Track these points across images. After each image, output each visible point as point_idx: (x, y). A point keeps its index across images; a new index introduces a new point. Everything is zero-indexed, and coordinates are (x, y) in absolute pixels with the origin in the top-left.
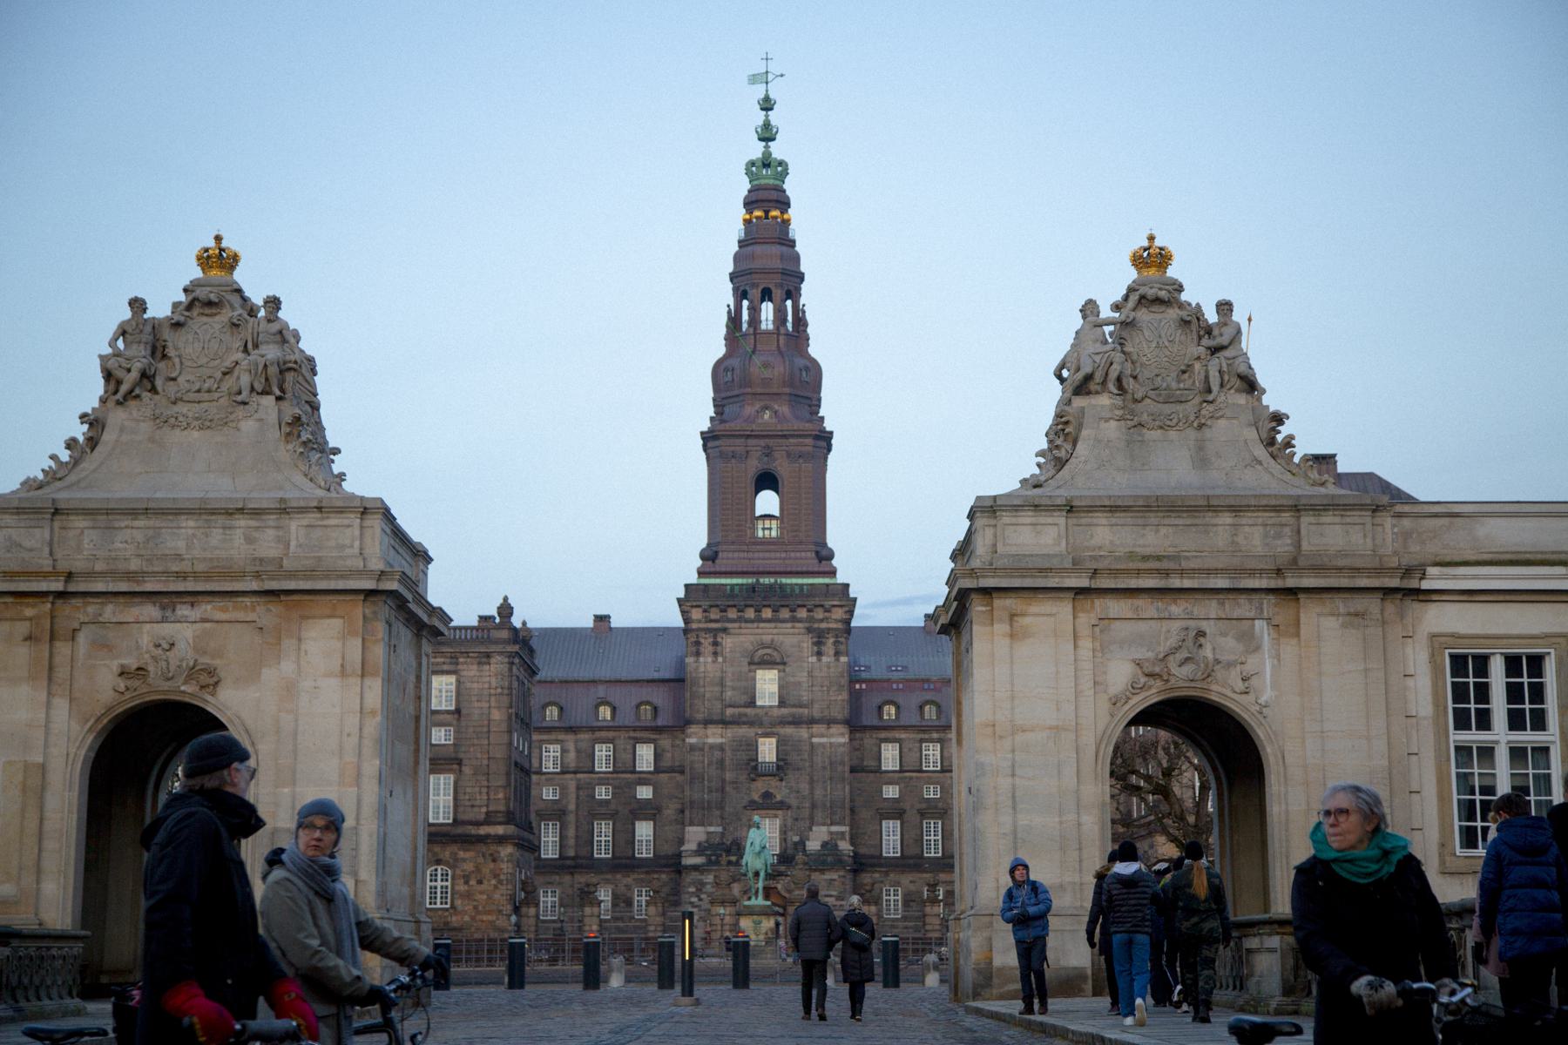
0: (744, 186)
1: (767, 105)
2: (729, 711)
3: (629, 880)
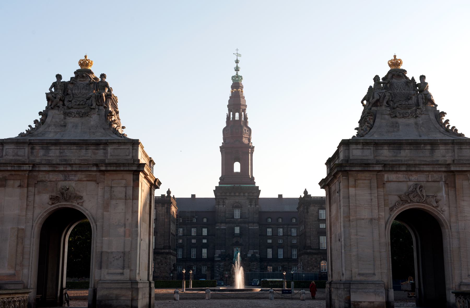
0: (231, 82)
1: (237, 62)
2: (227, 220)
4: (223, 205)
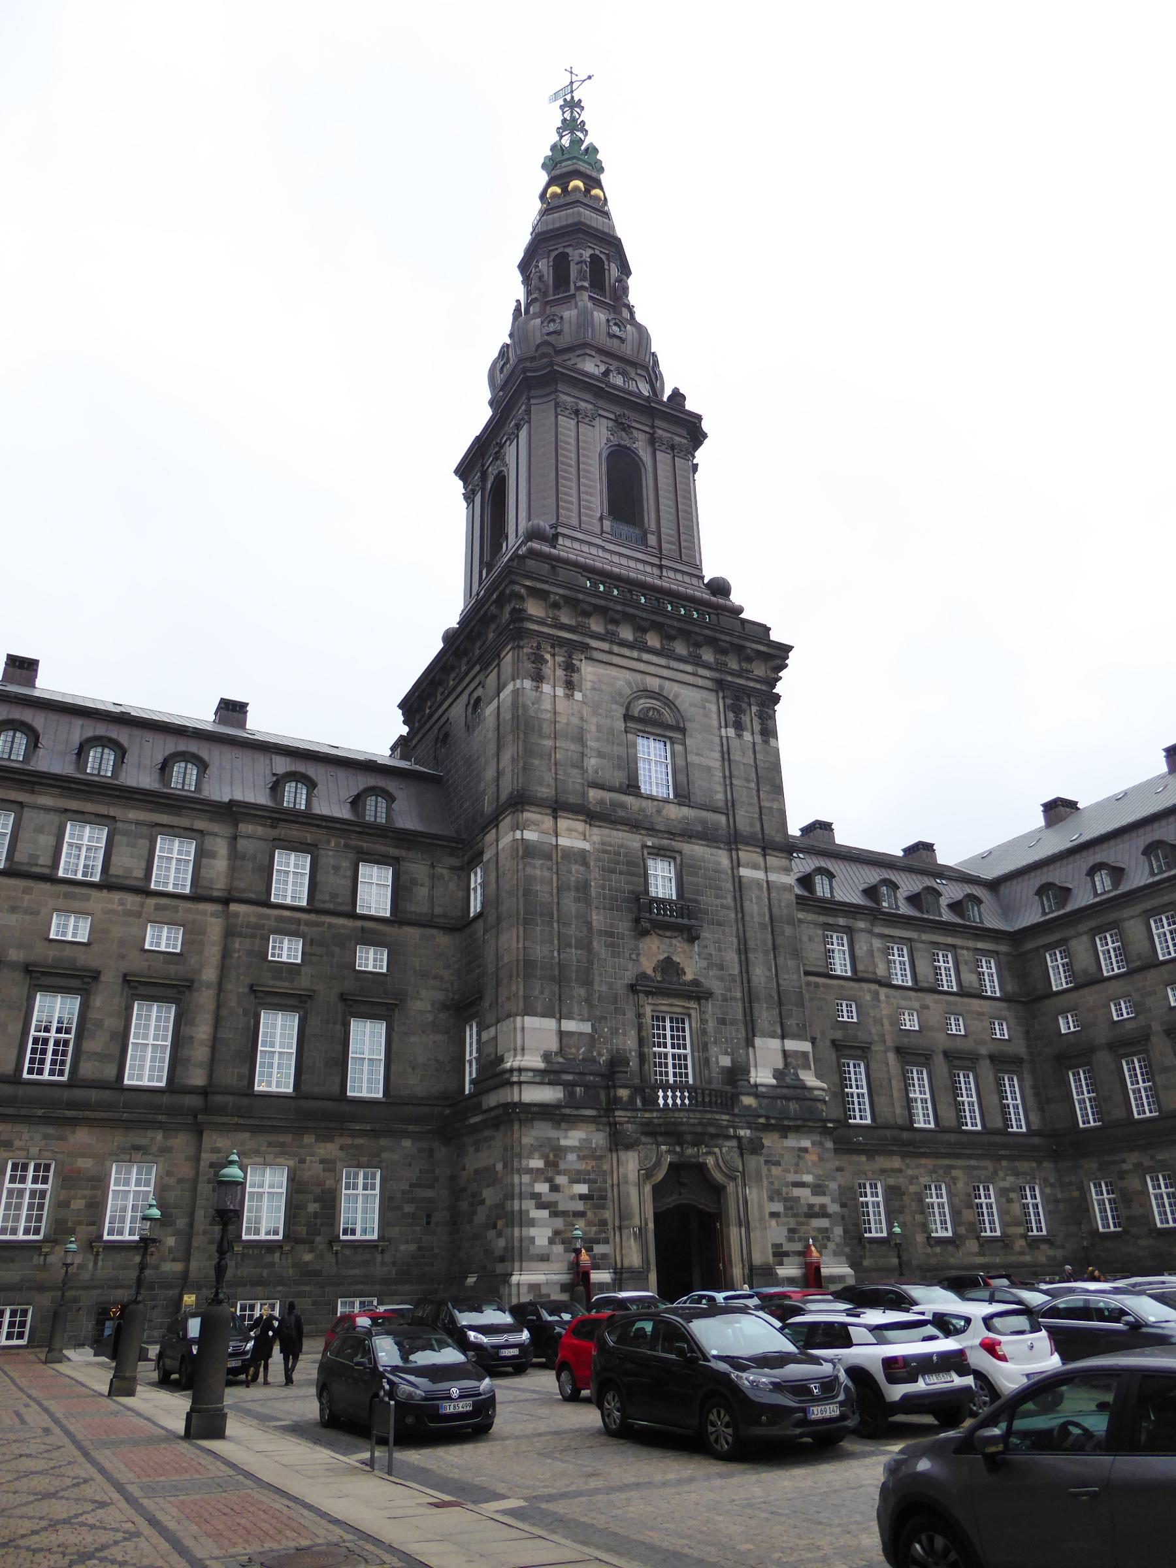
2: (594, 794)
3: (329, 1149)
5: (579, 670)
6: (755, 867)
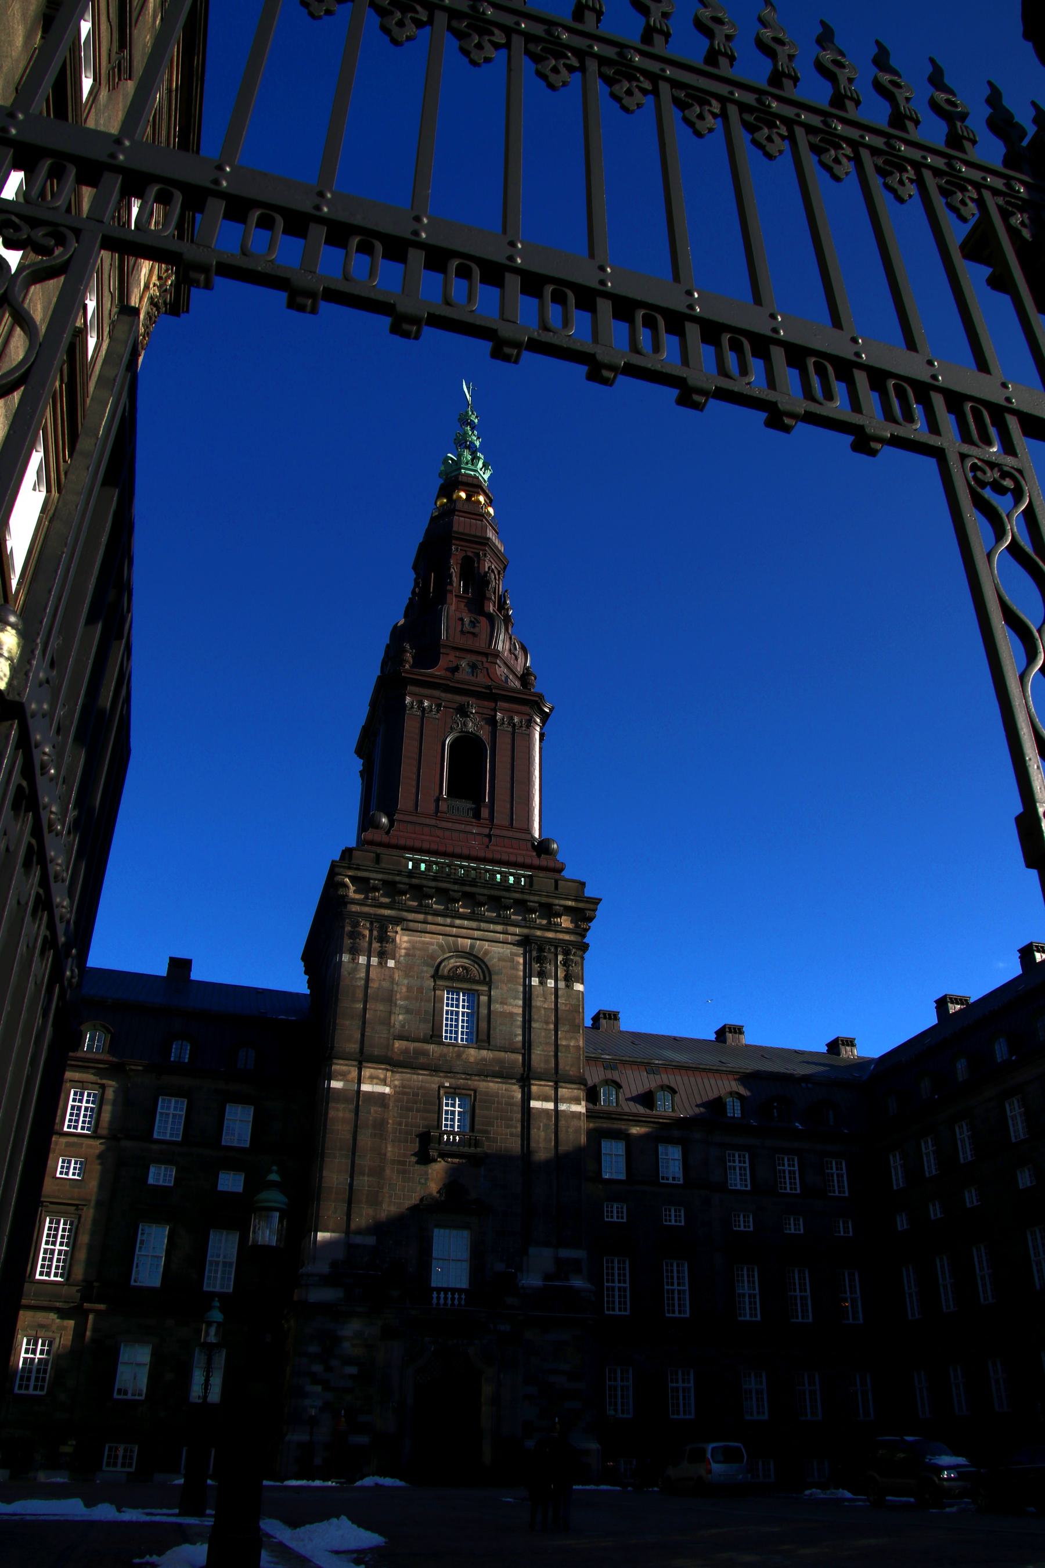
2: (397, 1044)
4: (383, 955)
5: (394, 940)
6: (546, 1099)
